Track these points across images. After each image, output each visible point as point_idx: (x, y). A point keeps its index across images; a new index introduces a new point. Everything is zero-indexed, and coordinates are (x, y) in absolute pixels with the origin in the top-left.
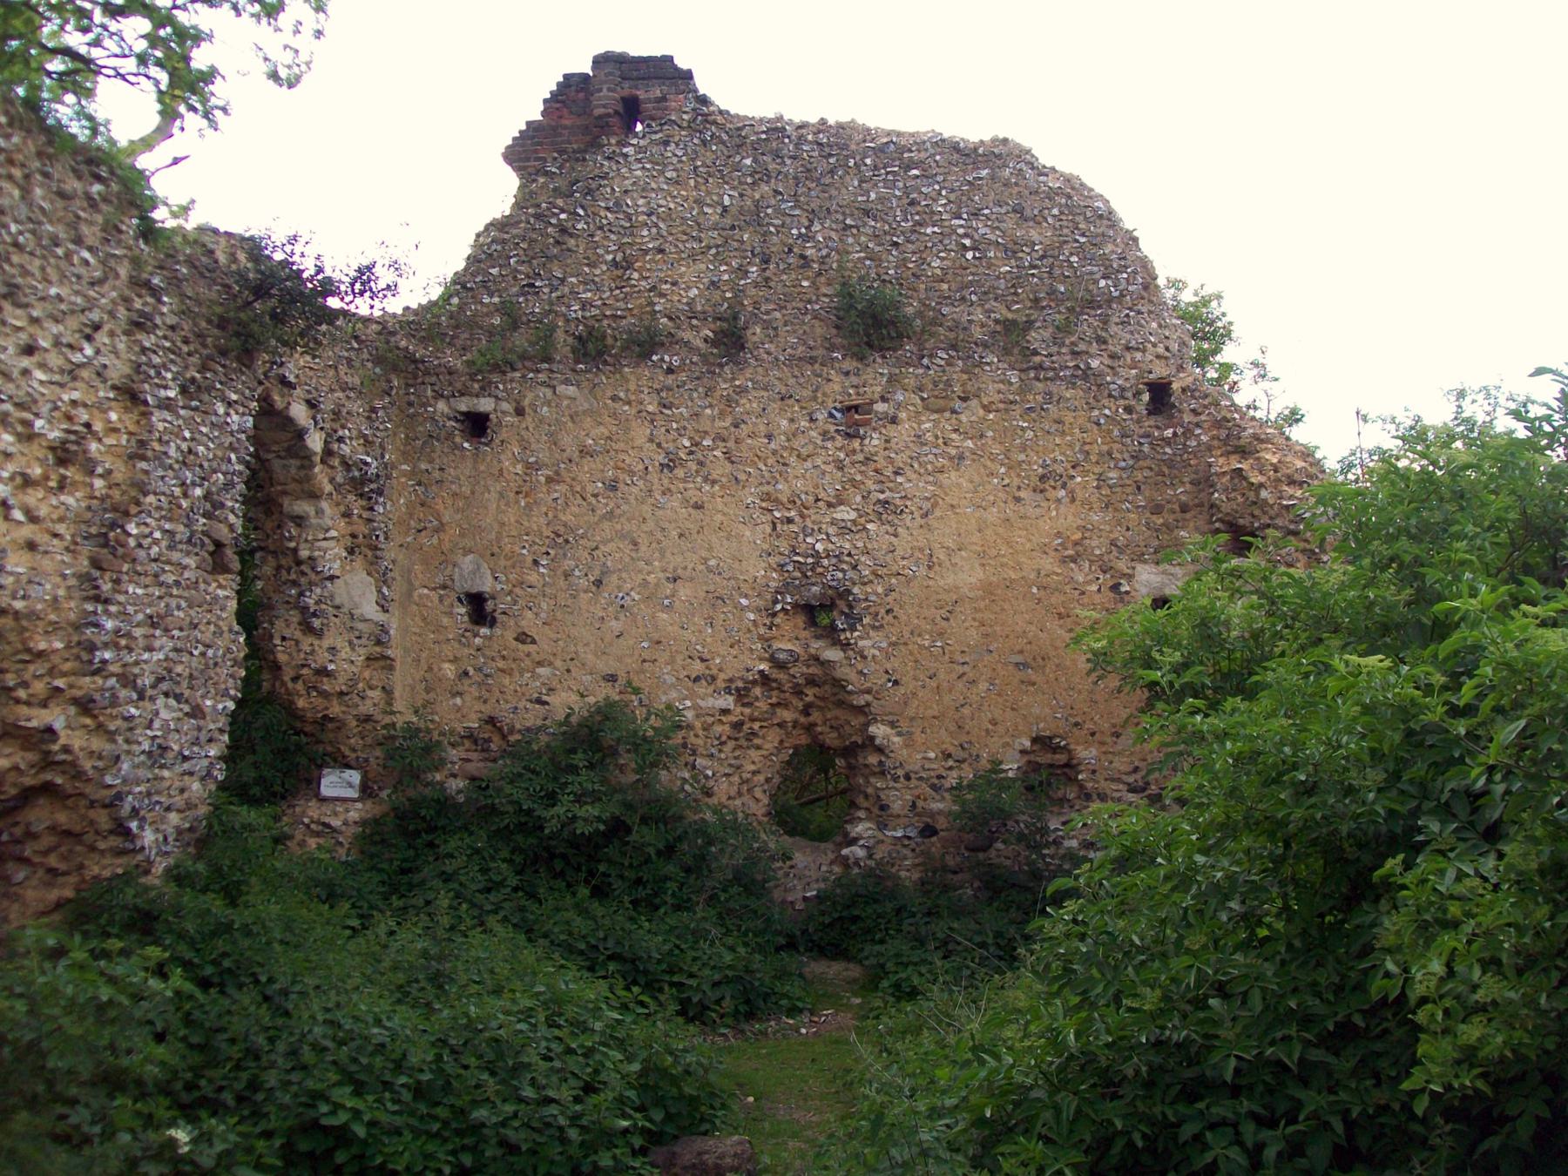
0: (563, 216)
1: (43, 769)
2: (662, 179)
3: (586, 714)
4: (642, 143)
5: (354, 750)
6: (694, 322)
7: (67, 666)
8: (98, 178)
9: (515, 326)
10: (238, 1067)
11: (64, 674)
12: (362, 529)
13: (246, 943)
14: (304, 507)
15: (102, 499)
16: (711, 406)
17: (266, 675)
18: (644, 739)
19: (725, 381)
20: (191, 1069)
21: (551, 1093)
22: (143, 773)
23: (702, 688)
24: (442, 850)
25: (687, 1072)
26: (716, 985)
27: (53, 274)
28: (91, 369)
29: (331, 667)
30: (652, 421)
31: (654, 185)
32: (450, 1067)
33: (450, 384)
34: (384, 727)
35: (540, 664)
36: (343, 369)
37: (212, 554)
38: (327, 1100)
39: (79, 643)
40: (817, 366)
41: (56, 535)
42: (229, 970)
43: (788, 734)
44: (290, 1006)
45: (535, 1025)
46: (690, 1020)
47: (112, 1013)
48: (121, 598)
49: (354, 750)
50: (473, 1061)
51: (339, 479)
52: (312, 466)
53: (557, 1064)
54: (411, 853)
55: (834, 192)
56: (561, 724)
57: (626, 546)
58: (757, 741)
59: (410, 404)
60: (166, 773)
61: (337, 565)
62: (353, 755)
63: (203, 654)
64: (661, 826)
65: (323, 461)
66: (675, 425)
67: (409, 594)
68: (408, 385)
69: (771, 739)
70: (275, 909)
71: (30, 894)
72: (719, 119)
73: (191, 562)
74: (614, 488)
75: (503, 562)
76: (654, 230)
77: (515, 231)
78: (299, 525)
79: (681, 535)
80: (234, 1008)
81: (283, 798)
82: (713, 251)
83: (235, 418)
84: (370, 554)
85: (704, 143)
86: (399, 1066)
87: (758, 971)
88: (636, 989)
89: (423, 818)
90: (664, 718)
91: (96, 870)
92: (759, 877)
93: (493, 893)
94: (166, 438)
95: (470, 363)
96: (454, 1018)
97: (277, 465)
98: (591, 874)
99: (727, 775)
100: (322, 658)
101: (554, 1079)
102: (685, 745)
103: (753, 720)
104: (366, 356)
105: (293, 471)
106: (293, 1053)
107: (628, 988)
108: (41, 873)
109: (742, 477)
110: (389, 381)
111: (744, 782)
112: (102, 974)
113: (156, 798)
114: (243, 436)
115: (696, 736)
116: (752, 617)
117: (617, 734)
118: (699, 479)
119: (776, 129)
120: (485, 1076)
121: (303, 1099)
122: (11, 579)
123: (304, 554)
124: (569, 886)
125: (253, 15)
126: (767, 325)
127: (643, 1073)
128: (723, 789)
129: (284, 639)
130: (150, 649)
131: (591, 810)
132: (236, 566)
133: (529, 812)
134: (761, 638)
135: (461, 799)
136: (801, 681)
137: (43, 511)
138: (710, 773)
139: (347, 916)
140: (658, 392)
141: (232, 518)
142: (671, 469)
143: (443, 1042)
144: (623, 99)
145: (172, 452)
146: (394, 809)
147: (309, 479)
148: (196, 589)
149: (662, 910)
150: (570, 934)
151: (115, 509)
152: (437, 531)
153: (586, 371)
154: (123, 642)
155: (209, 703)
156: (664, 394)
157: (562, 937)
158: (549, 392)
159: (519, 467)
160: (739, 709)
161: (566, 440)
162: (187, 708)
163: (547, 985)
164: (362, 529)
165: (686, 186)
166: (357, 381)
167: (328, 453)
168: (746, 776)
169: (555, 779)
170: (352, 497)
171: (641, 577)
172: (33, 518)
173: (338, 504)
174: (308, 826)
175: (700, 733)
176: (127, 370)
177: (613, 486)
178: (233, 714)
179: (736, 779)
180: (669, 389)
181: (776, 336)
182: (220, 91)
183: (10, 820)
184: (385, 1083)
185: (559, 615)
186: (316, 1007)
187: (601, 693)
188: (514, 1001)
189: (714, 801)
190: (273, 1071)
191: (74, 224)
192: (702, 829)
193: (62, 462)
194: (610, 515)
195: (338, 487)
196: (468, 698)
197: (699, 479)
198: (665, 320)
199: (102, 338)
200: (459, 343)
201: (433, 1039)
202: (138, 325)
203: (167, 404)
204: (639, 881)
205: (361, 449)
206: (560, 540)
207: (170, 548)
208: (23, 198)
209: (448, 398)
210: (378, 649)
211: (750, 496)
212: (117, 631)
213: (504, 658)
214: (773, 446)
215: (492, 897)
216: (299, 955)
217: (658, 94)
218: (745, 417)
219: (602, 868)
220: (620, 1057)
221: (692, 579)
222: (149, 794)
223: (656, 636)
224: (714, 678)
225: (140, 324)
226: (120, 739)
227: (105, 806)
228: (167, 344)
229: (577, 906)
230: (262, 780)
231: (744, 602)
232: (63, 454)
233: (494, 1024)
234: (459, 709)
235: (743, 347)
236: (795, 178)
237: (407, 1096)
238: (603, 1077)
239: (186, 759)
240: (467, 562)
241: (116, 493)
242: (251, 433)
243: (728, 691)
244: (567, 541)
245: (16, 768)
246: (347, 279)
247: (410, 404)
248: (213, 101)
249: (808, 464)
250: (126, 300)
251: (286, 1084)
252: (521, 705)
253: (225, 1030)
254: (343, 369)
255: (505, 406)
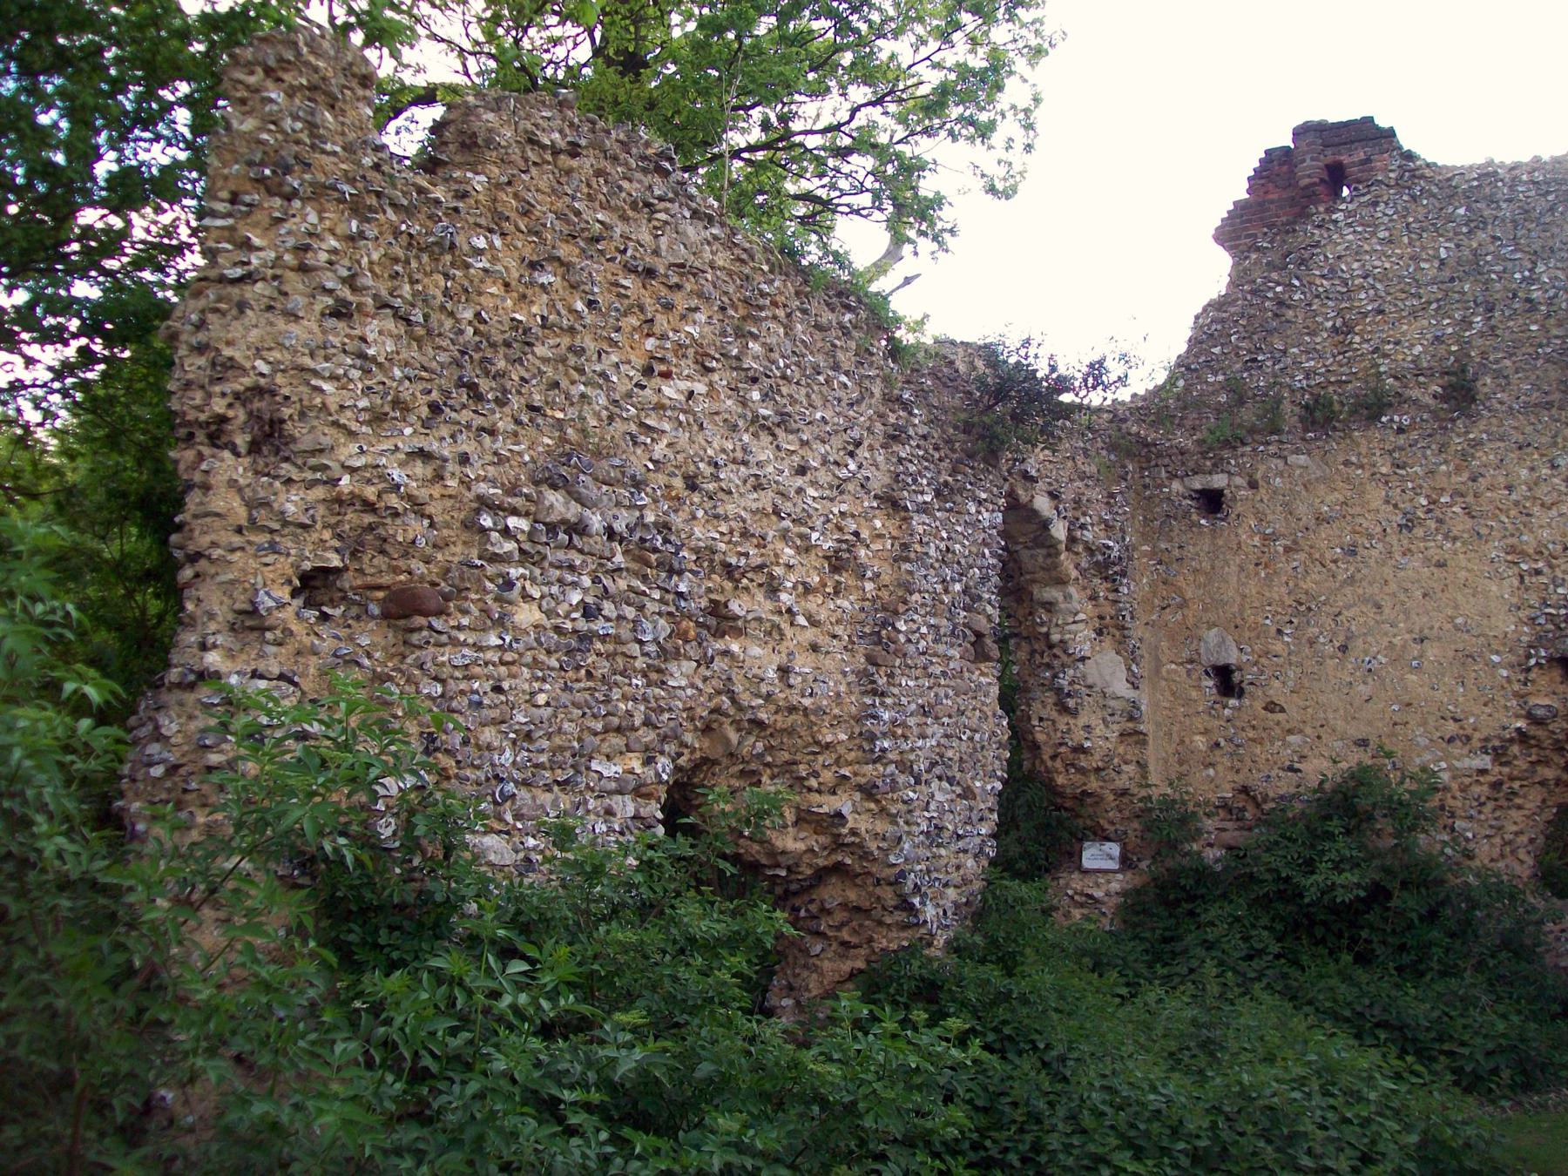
0: (1279, 289)
1: (833, 851)
2: (1374, 240)
3: (1339, 780)
4: (1351, 207)
5: (1113, 823)
6: (1421, 379)
7: (852, 756)
8: (848, 308)
9: (1241, 402)
10: (1021, 1130)
11: (849, 764)
12: (1109, 610)
13: (1025, 1011)
14: (1052, 594)
15: (873, 601)
16: (1446, 462)
17: (1026, 755)
18: (1400, 803)
19: (1459, 436)
20: (977, 1130)
21: (1329, 1163)
22: (923, 852)
23: (1456, 748)
24: (1204, 918)
25: (1467, 1145)
26: (1489, 1054)
27: (818, 401)
28: (856, 482)
29: (1087, 744)
30: (1387, 483)
31: (1367, 247)
32: (1226, 1135)
33: (1183, 464)
34: (1141, 800)
35: (1290, 732)
36: (1080, 459)
37: (973, 644)
38: (1108, 1163)
39: (861, 734)
40: (1554, 411)
41: (835, 637)
42: (1010, 1038)
43: (1550, 792)
44: (1068, 1073)
45: (1309, 1094)
46: (1467, 1090)
47: (917, 1080)
48: (896, 691)
49: (1113, 823)
50: (1250, 1128)
51: (1084, 564)
52: (1058, 554)
53: (1333, 1133)
54: (1173, 921)
55: (1556, 230)
56: (1315, 791)
57: (1370, 610)
58: (1518, 801)
59: (1146, 487)
60: (943, 852)
61: (1087, 646)
62: (1112, 828)
63: (971, 739)
64: (1423, 890)
65: (1068, 549)
66: (1410, 485)
67: (1157, 671)
68: (1142, 469)
69: (1533, 798)
70: (1049, 978)
71: (826, 965)
72: (1427, 172)
73: (955, 653)
74: (1354, 553)
75: (1247, 634)
76: (1372, 292)
77: (1233, 310)
78: (1049, 611)
79: (1425, 595)
80: (1015, 1073)
81: (1047, 871)
82: (1434, 306)
83: (986, 515)
84: (1117, 634)
85: (1414, 198)
86: (1176, 1132)
87: (1535, 1040)
88: (1409, 1059)
89: (1183, 888)
90: (1419, 781)
91: (884, 943)
92: (1528, 942)
93: (1256, 960)
94: (925, 540)
95: (1200, 442)
96: (1228, 1086)
97: (1025, 555)
98: (1354, 940)
99: (1487, 837)
100: (1078, 736)
101: (1331, 1148)
102: (1442, 808)
103: (1512, 779)
104: (1100, 445)
105: (1040, 559)
106: (1072, 1117)
107: (1400, 1057)
108: (835, 945)
109: (1484, 531)
110: (1124, 467)
111: (1506, 843)
112: (909, 1043)
113: (935, 875)
114: (994, 532)
115: (1454, 798)
116: (1505, 673)
117: (1371, 800)
118: (1439, 537)
119: (1488, 175)
120: (1262, 1144)
121: (1085, 1162)
122: (800, 679)
123: (1055, 637)
124: (1331, 953)
125: (968, 138)
126: (1498, 374)
127: (1422, 1145)
128: (1484, 851)
129: (1041, 719)
130: (923, 736)
131: (1350, 877)
132: (996, 653)
133: (1288, 879)
134: (1516, 695)
135: (1218, 867)
136: (1561, 737)
137: (823, 616)
138: (1470, 835)
139: (1115, 985)
140: (1390, 452)
141: (989, 609)
142: (1410, 530)
143: (1217, 1109)
144: (1327, 166)
145: (932, 552)
146: (1154, 879)
147: (1056, 566)
148: (962, 678)
149: (1429, 977)
150: (1335, 1001)
151: (884, 609)
152: (1181, 606)
153: (1316, 439)
154: (899, 731)
155: (978, 784)
156: (1396, 455)
157: (1328, 1004)
158: (1280, 463)
159: (1257, 539)
160: (1497, 769)
161: (1302, 509)
162: (959, 790)
163: (1318, 1054)
164: (1109, 610)
165: (1400, 246)
166: (1094, 469)
167: (1072, 540)
168: (1508, 837)
169: (1312, 846)
170: (1097, 581)
171: (1386, 640)
172: (814, 622)
173: (1085, 588)
174: (1072, 898)
175: (1458, 794)
176: (887, 480)
177: (1352, 551)
178: (1000, 794)
179: (1497, 840)
180: (1402, 449)
181: (1509, 384)
182: (946, 215)
183: (806, 898)
184: (1162, 1149)
185: (1306, 682)
186: (1092, 1074)
187: (1354, 758)
188: (1286, 1069)
189: (1477, 863)
190: (1056, 1134)
191: (832, 352)
192: (1465, 892)
193: (835, 569)
194: (1351, 580)
195: (1083, 572)
196: (1220, 768)
197: (1439, 537)
198: (1390, 380)
199: (863, 453)
200: (1188, 423)
201: (1207, 1106)
202: (894, 438)
203: (924, 509)
204: (1402, 948)
205: (1102, 534)
206: (1303, 608)
207: (935, 641)
208: (786, 334)
209: (1182, 478)
210: (1130, 725)
211: (1494, 550)
212: (893, 722)
213: (1254, 727)
214: (1514, 497)
215: (1254, 964)
216: (1073, 1023)
217: (1362, 156)
218: (1482, 470)
219: (1364, 934)
220: (1397, 1128)
221: (1439, 639)
222: (929, 871)
223: (1406, 698)
224: (1469, 738)
225: (896, 436)
226: (901, 822)
227: (890, 884)
228: (921, 453)
229: (1340, 973)
230: (1026, 855)
231: (1495, 658)
232: (837, 562)
233: (1268, 1092)
234: (1212, 780)
235: (1473, 400)
236: (1513, 221)
237: (1185, 1162)
238: (1381, 1147)
239: (959, 837)
240: (1212, 636)
241: (885, 594)
242: (1001, 528)
243: (1484, 750)
244: (1309, 609)
245: (811, 850)
246: (1078, 375)
247: (1146, 487)
248: (939, 225)
249: (1554, 512)
250: (881, 416)
251: (1067, 1148)
252: (1273, 774)
253: (1008, 1094)
254: (1080, 459)
255: (1238, 480)
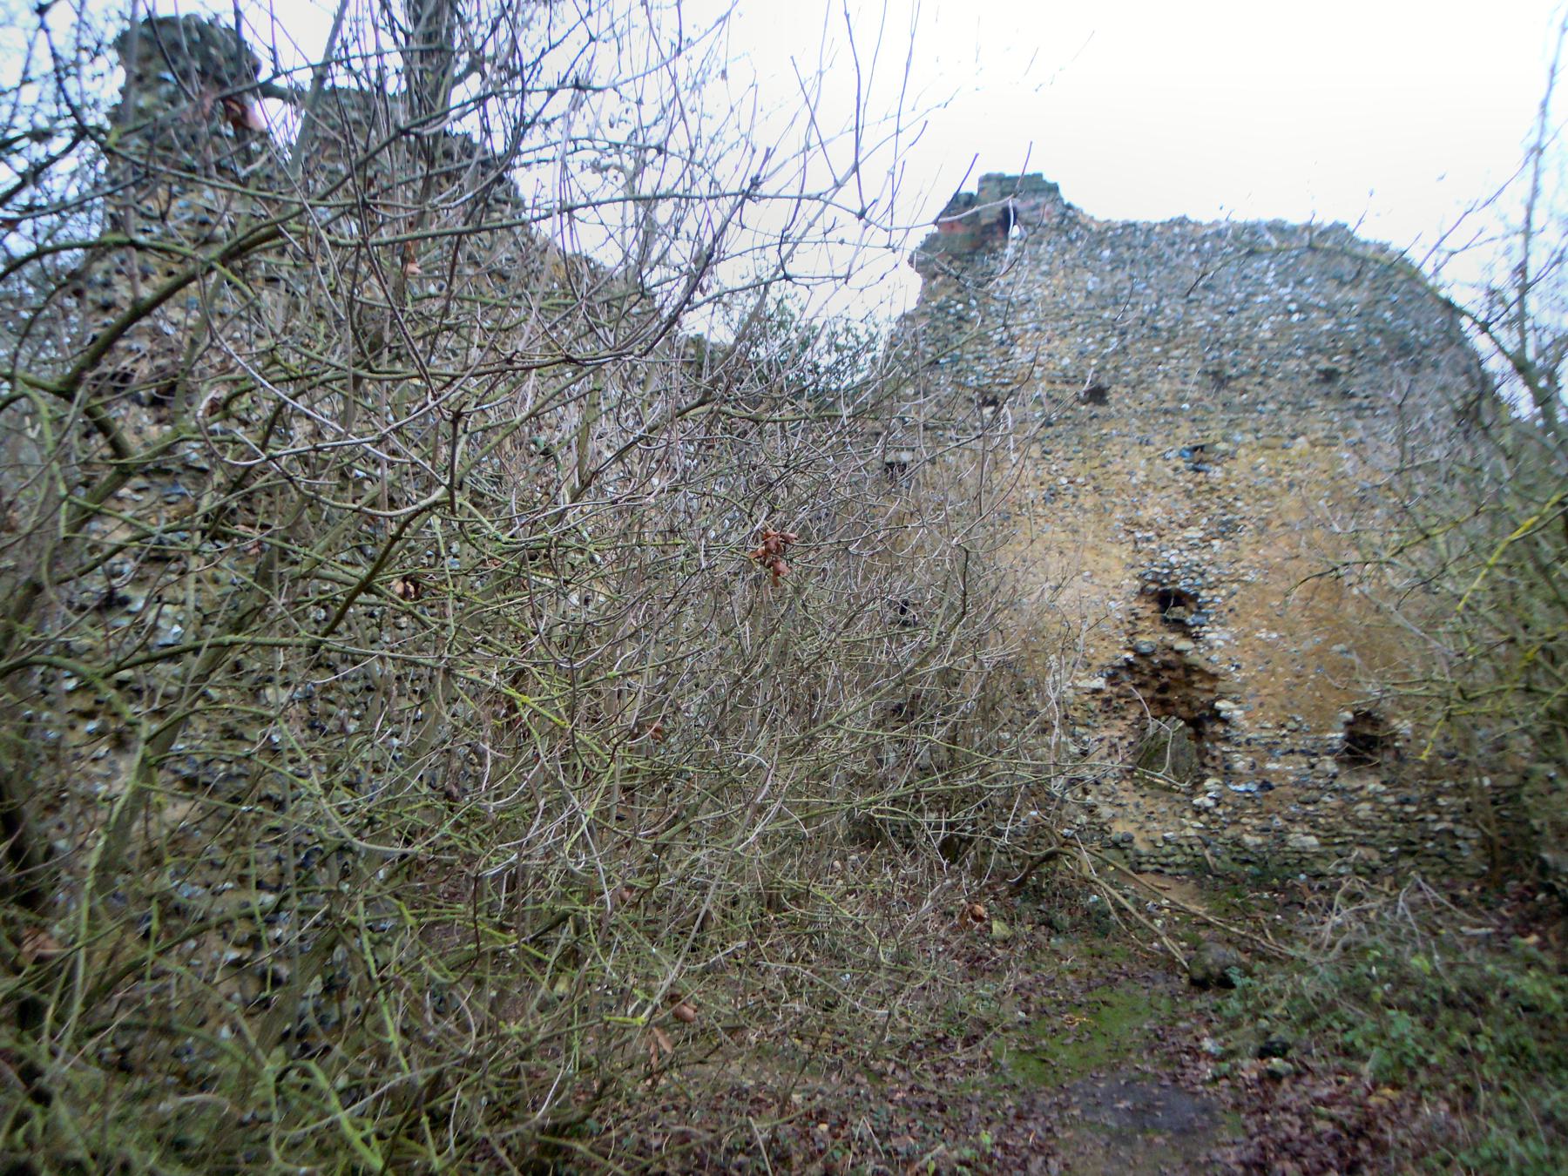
85: (1070, 241)
103: (1119, 696)
214: (1134, 480)
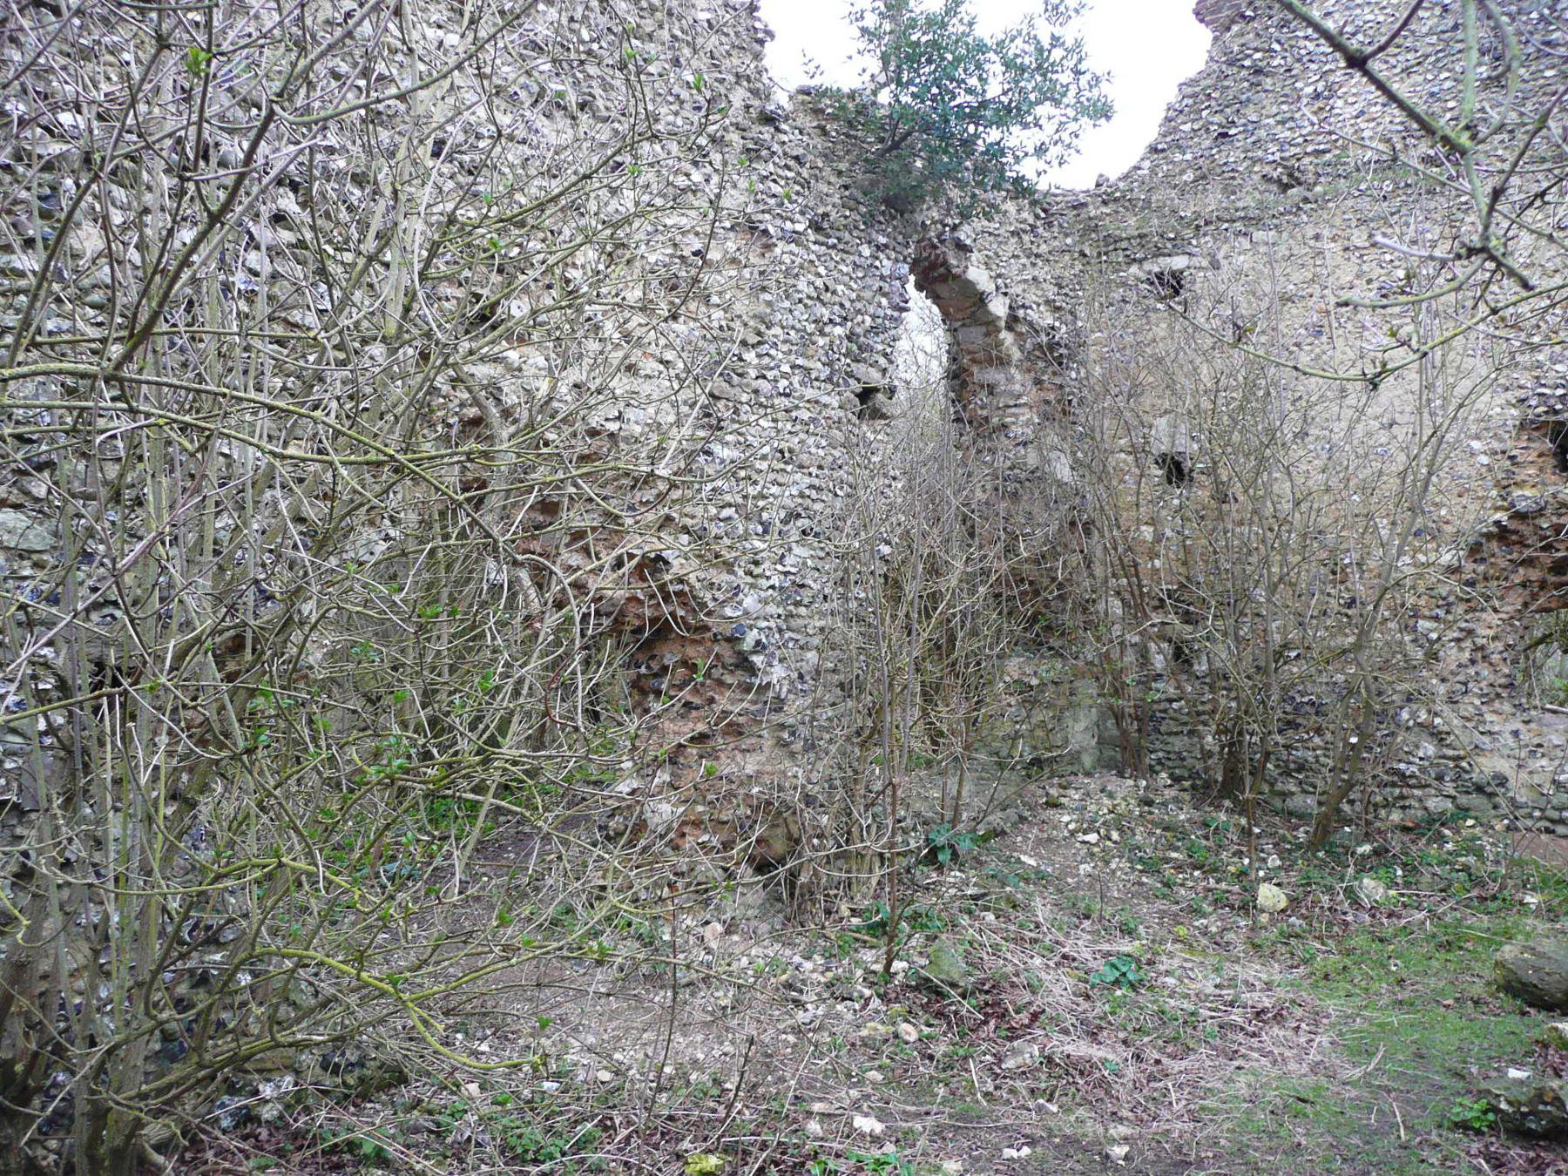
0: (1258, 55)
82: (1432, 59)
168: (1480, 641)
179: (1468, 644)
